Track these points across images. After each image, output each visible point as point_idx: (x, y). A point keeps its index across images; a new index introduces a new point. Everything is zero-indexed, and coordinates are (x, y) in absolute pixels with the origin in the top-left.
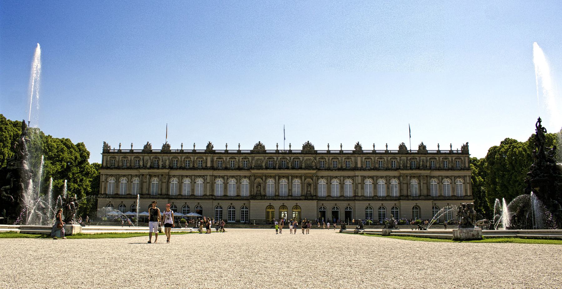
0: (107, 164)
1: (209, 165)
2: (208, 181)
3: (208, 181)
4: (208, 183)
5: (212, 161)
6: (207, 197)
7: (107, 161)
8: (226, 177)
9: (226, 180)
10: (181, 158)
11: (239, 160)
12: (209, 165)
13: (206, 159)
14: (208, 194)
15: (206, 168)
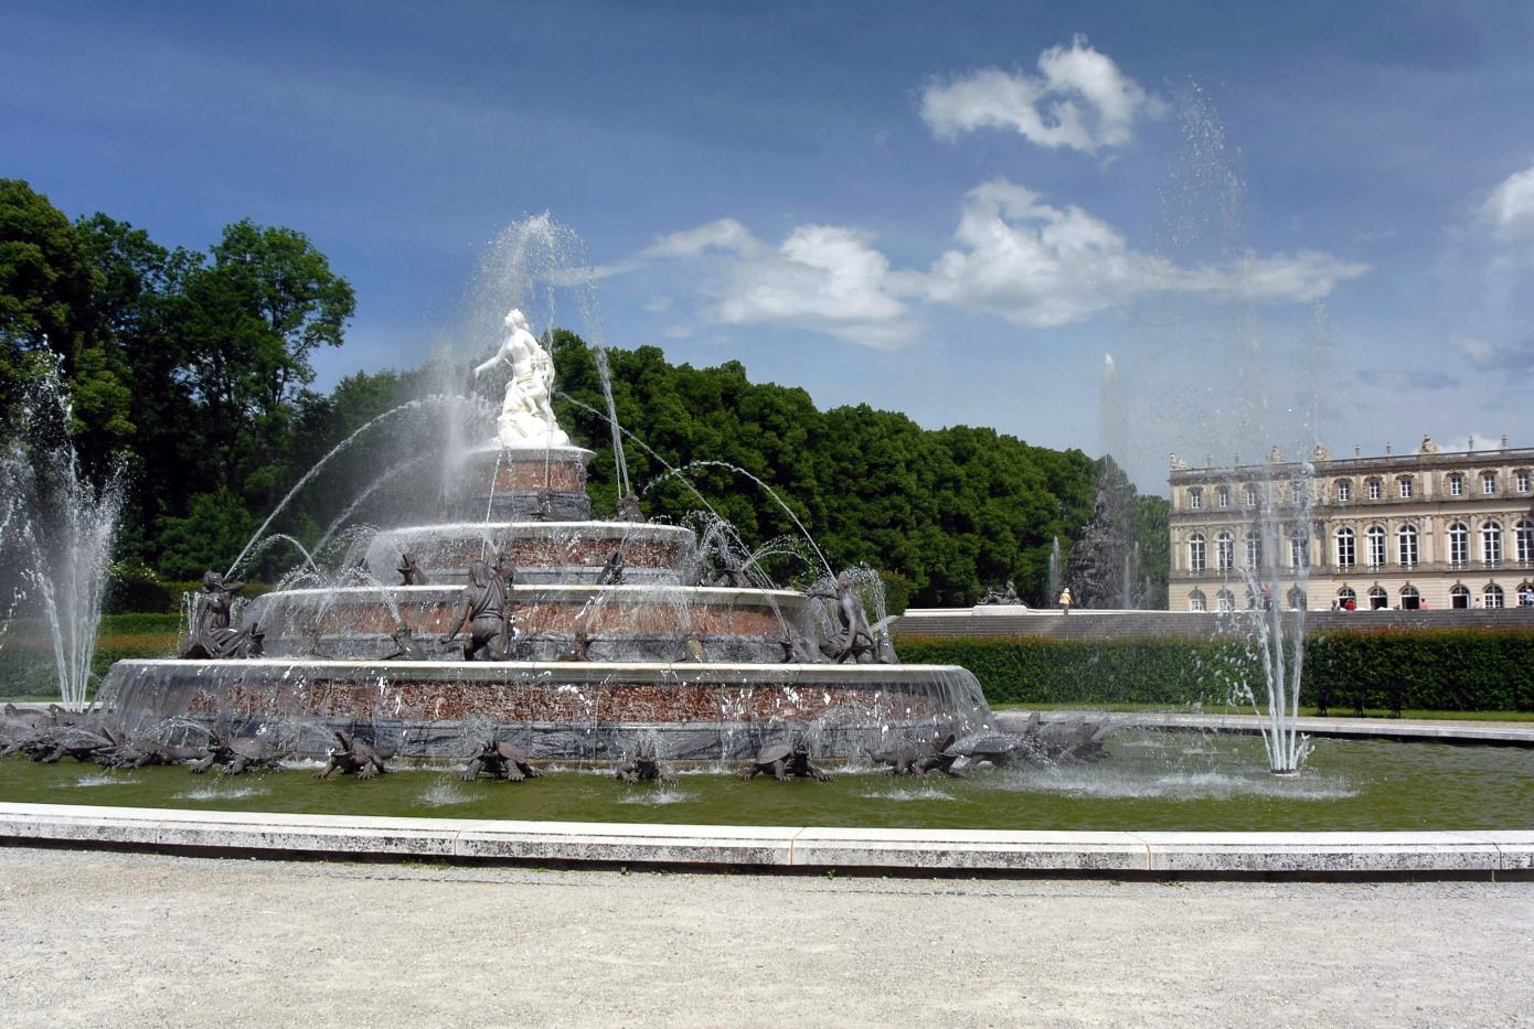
0: (1182, 503)
1: (1428, 490)
2: (1428, 528)
3: (1428, 528)
4: (1428, 534)
5: (1435, 482)
6: (1427, 568)
7: (1181, 498)
8: (1473, 518)
9: (1473, 525)
10: (1358, 480)
11: (1505, 474)
12: (1428, 490)
13: (1421, 478)
14: (1430, 559)
15: (1421, 504)
